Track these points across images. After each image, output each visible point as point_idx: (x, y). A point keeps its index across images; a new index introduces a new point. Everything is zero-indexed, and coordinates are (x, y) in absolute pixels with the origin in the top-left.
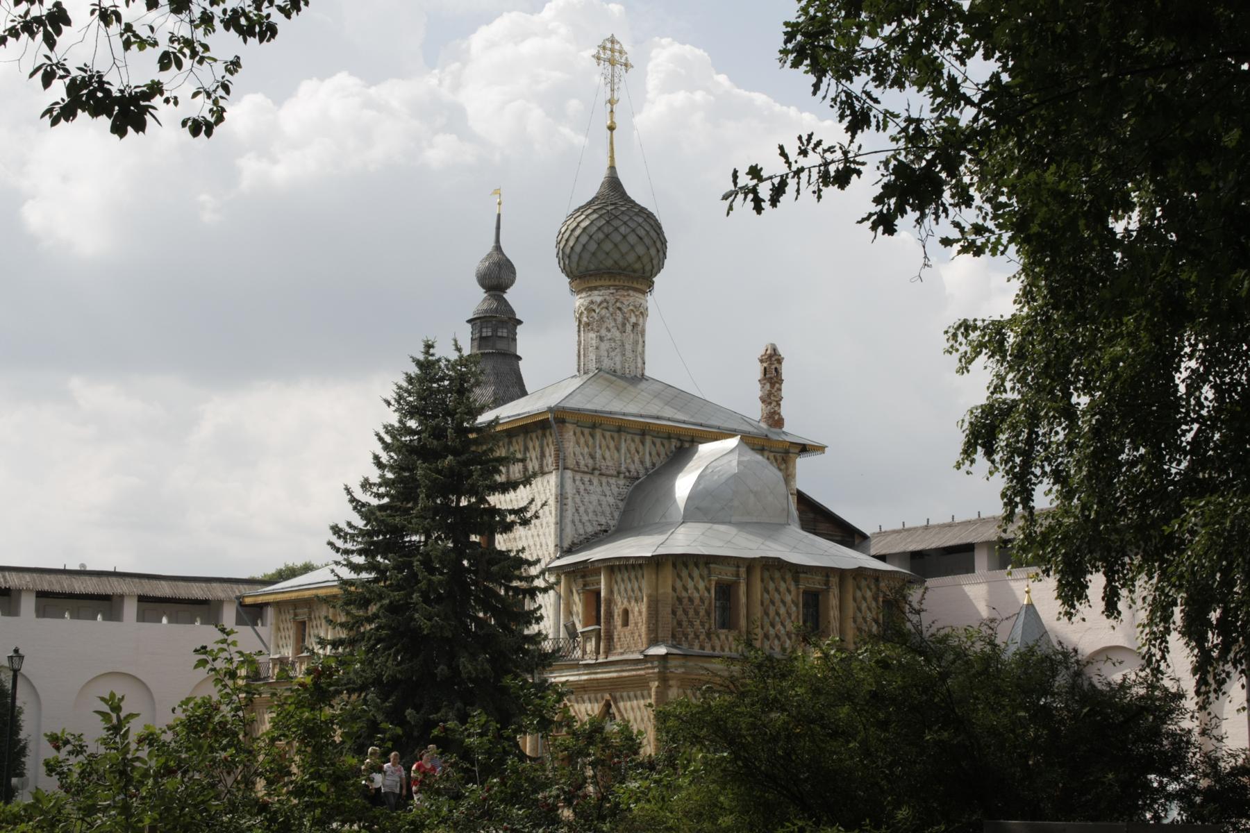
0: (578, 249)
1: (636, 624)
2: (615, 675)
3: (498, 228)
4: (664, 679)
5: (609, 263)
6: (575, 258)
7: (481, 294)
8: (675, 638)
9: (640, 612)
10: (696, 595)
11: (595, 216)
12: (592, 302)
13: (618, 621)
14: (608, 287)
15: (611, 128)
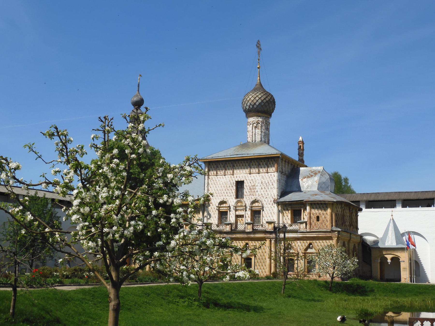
0: (257, 104)
1: (323, 221)
2: (316, 235)
3: (139, 87)
4: (338, 238)
5: (266, 109)
6: (255, 106)
7: (132, 108)
8: (337, 226)
9: (325, 217)
10: (339, 213)
11: (262, 94)
12: (259, 121)
13: (314, 219)
14: (263, 117)
15: (259, 68)
